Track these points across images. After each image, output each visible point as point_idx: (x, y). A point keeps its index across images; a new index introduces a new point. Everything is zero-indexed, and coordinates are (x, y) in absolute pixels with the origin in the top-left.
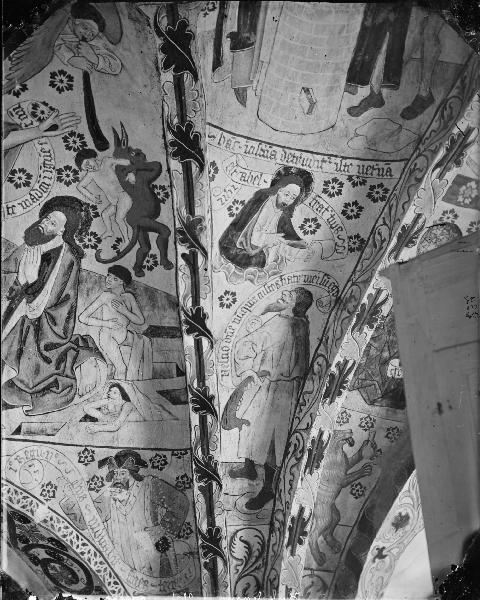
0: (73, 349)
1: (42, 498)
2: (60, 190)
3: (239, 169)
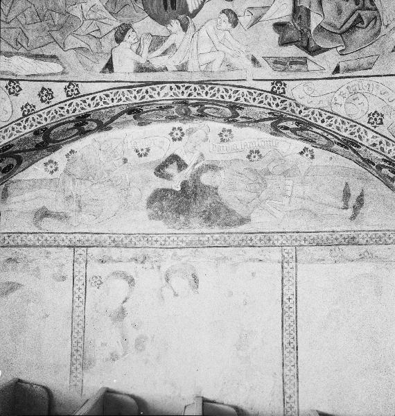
1: (369, 126)
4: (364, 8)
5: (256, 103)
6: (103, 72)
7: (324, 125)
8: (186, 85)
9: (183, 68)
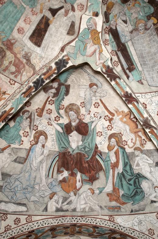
0: (136, 178)
1: (150, 235)
2: (110, 132)
3: (153, 102)
4: (137, 188)
5: (104, 225)
6: (43, 211)
7: (132, 235)
8: (76, 217)
9: (74, 210)
